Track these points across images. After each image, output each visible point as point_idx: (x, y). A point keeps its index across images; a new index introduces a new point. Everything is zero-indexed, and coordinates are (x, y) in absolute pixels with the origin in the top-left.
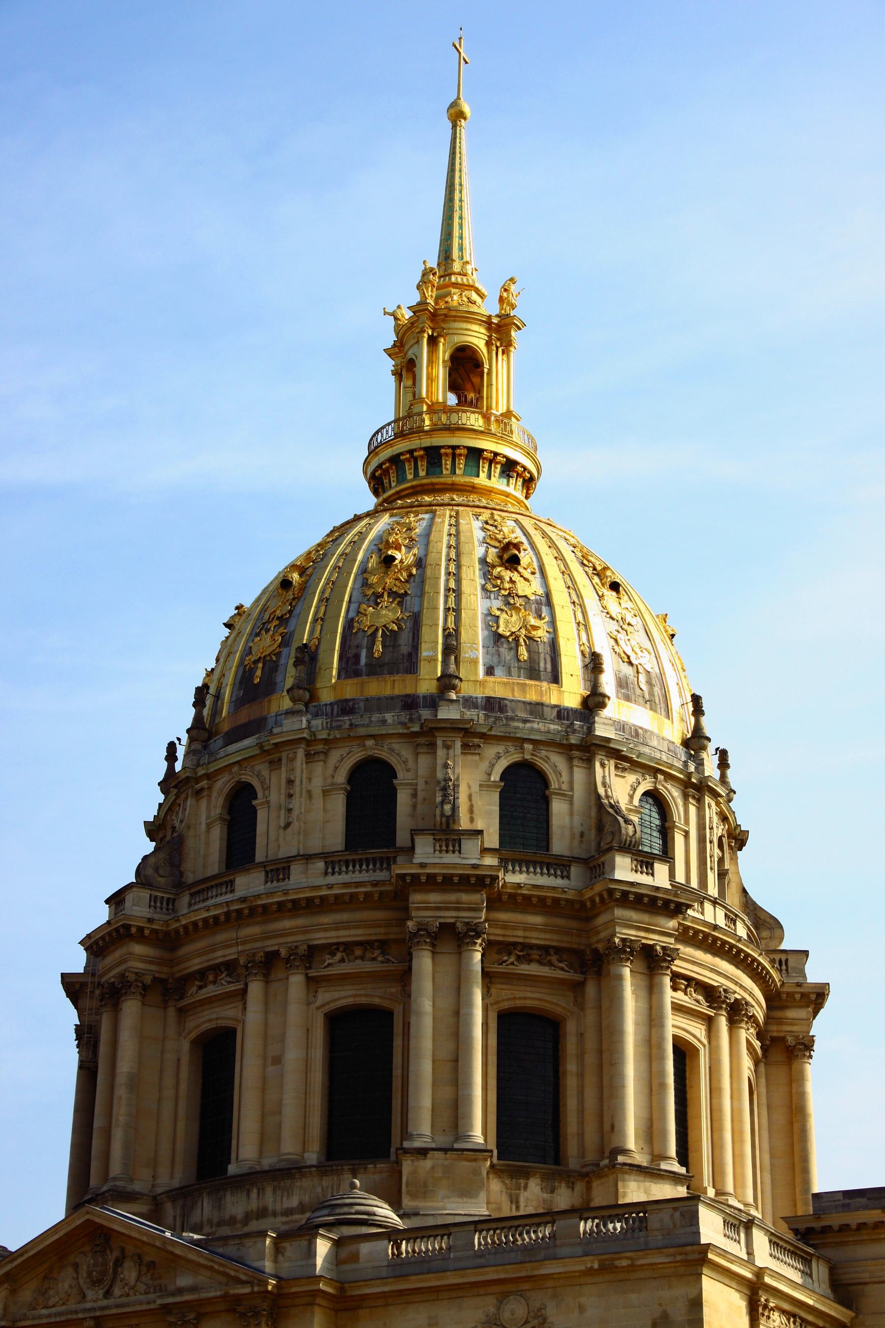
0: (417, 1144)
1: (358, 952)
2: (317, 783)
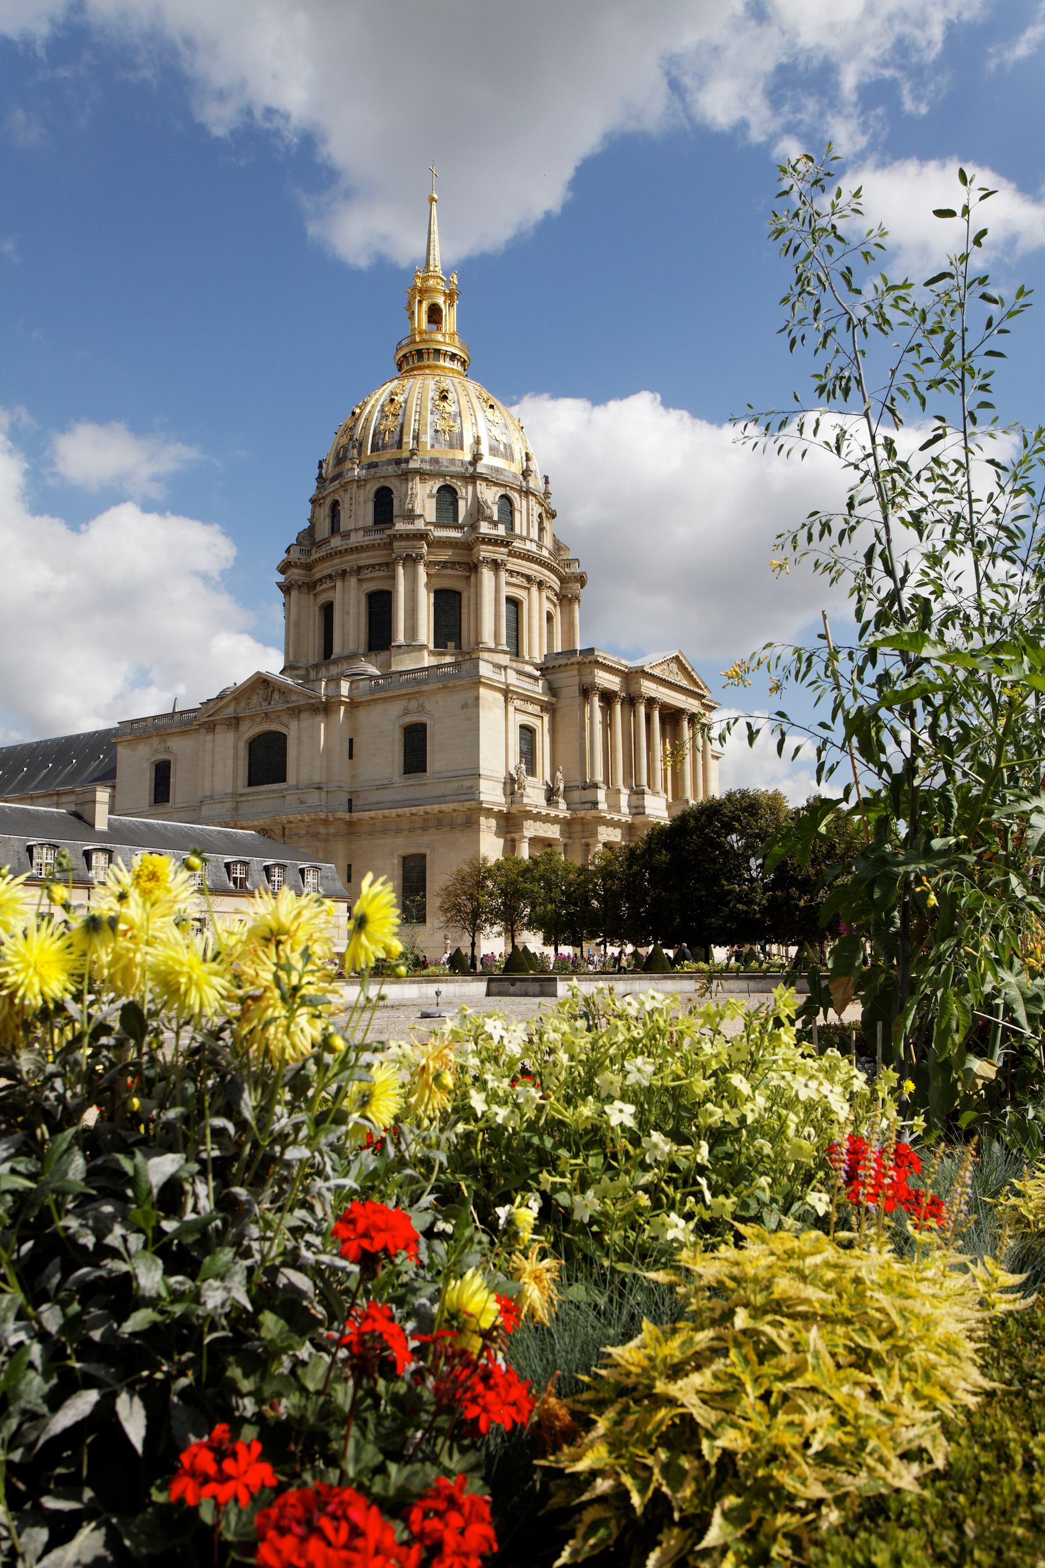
2: (362, 499)
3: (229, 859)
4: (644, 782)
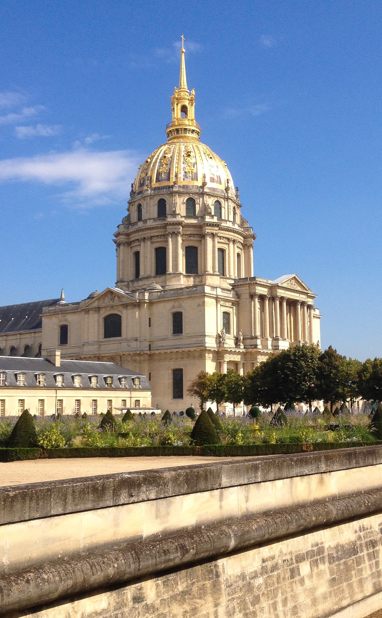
0: (169, 273)
1: (159, 237)
2: (152, 205)
3: (105, 376)
4: (279, 335)
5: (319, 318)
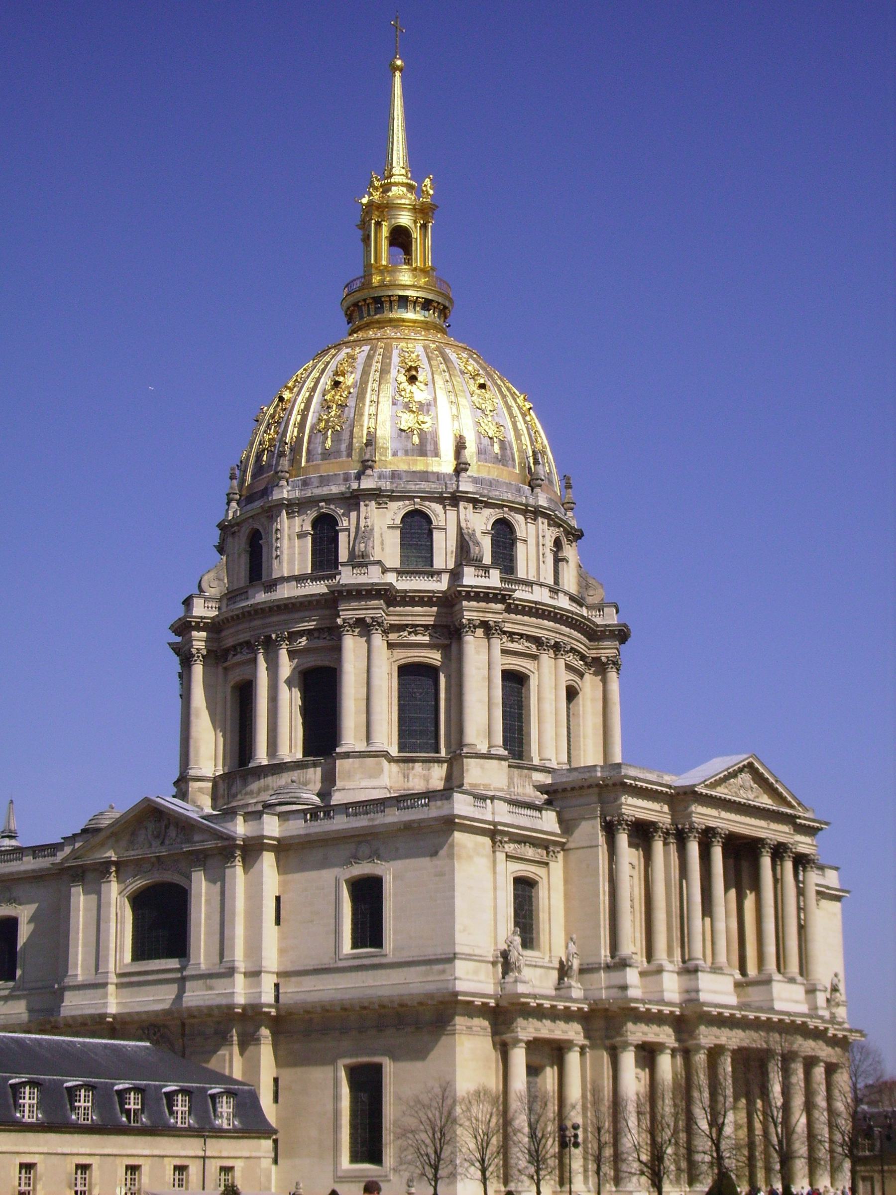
1: (316, 635)
5: (838, 898)
